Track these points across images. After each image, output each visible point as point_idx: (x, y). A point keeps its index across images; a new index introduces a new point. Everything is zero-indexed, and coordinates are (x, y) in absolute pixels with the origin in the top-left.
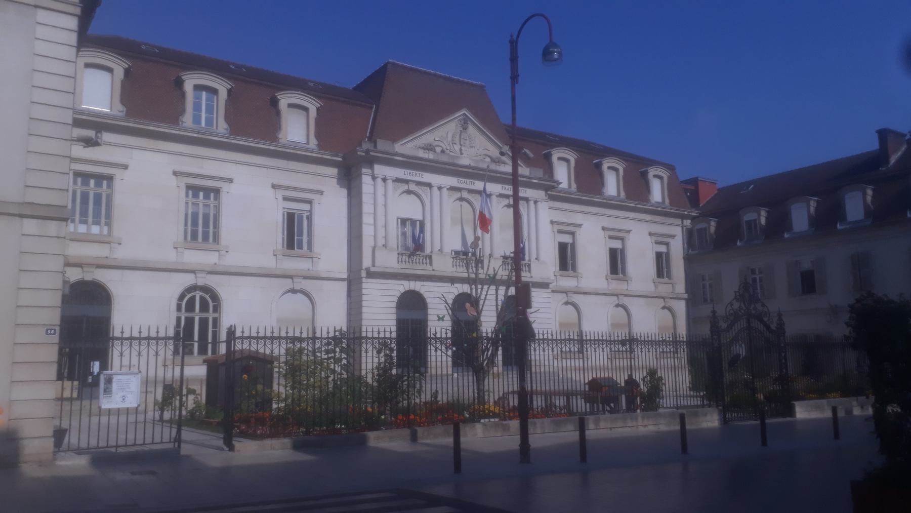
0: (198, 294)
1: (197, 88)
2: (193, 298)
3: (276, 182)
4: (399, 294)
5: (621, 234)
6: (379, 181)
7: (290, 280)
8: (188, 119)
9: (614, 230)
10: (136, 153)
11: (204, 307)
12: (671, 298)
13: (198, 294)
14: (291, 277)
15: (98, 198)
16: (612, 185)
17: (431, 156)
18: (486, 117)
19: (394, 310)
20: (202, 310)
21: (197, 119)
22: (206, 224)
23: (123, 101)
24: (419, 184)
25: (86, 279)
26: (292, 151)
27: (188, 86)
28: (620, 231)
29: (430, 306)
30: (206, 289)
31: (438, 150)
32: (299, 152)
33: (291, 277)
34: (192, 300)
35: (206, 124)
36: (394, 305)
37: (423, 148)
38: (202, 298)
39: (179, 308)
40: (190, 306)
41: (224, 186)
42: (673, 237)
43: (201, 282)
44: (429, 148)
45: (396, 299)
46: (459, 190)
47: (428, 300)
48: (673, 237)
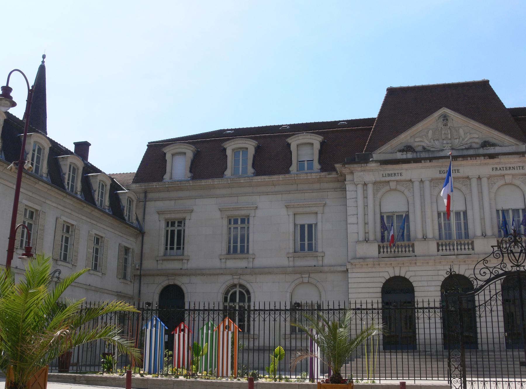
0: (238, 289)
1: (236, 152)
2: (235, 292)
4: (384, 281)
6: (360, 187)
10: (199, 201)
11: (242, 299)
13: (238, 289)
15: (179, 232)
17: (410, 155)
19: (380, 295)
20: (240, 301)
22: (242, 241)
23: (191, 171)
25: (170, 283)
29: (416, 289)
30: (241, 286)
31: (420, 149)
34: (234, 294)
36: (380, 290)
37: (400, 151)
38: (241, 293)
39: (226, 299)
40: (233, 299)
41: (252, 213)
43: (236, 282)
45: (381, 285)
47: (414, 284)
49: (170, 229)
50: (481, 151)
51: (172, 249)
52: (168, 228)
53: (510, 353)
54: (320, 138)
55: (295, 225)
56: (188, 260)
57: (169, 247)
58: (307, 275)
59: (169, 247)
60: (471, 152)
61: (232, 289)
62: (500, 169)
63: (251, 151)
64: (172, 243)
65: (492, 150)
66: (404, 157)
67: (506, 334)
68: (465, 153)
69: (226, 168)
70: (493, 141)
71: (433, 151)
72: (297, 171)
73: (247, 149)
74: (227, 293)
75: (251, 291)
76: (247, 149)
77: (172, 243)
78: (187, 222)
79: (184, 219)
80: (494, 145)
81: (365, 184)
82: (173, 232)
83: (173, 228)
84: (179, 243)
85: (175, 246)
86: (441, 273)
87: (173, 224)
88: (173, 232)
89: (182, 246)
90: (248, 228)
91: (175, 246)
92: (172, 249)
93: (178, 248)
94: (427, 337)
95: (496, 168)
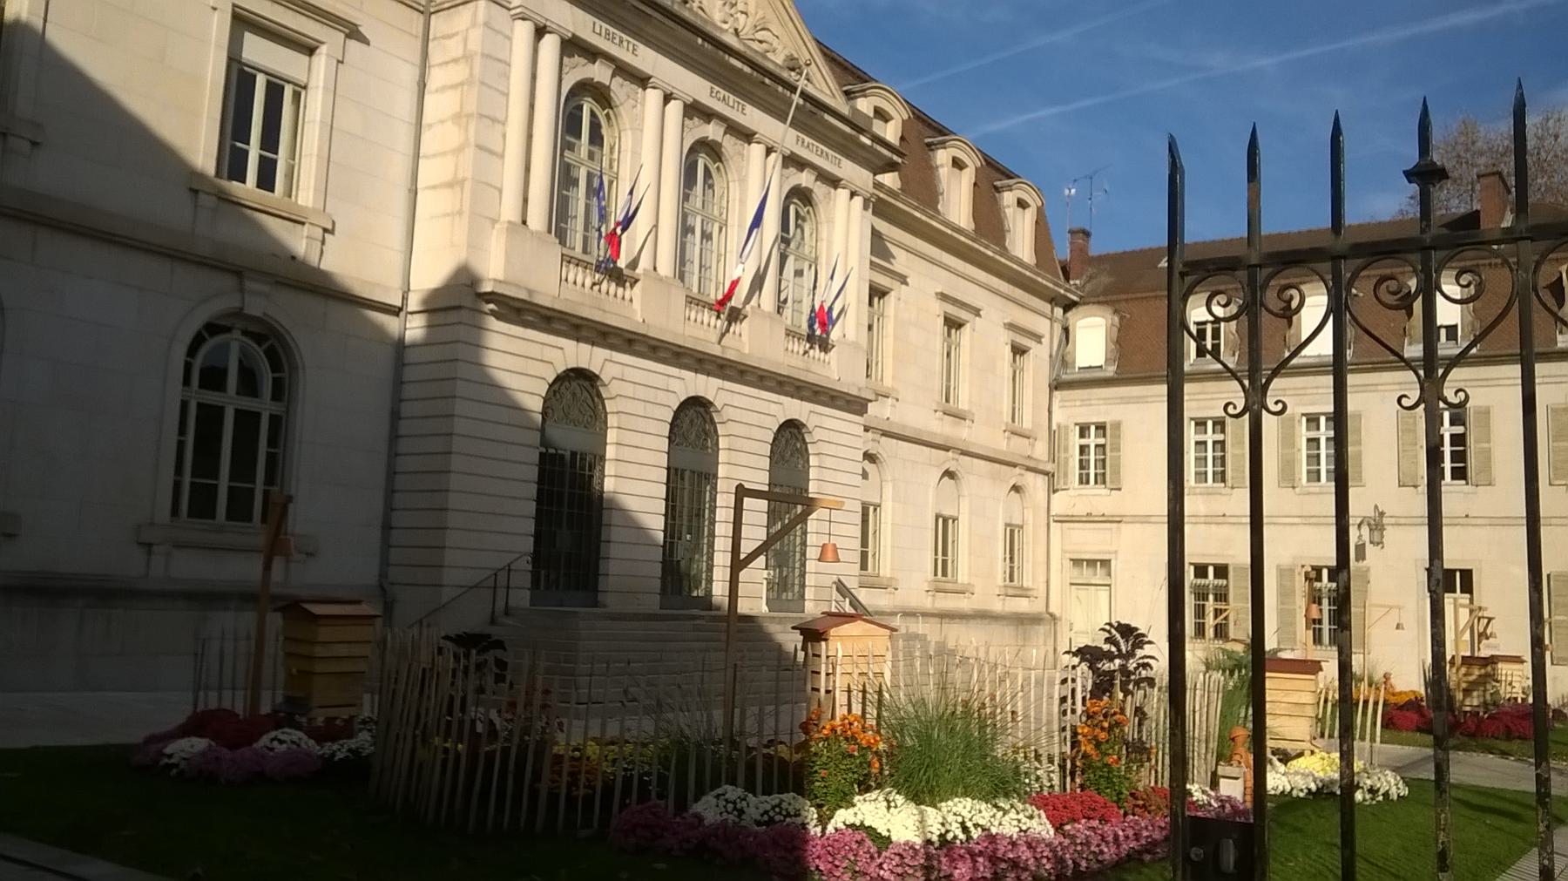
5: (963, 315)
7: (229, 282)
12: (1028, 469)
14: (238, 273)
16: (957, 201)
24: (623, 70)
33: (238, 273)
42: (1038, 338)
46: (708, 115)
48: (1038, 338)
55: (234, 60)
81: (540, 32)
86: (675, 385)
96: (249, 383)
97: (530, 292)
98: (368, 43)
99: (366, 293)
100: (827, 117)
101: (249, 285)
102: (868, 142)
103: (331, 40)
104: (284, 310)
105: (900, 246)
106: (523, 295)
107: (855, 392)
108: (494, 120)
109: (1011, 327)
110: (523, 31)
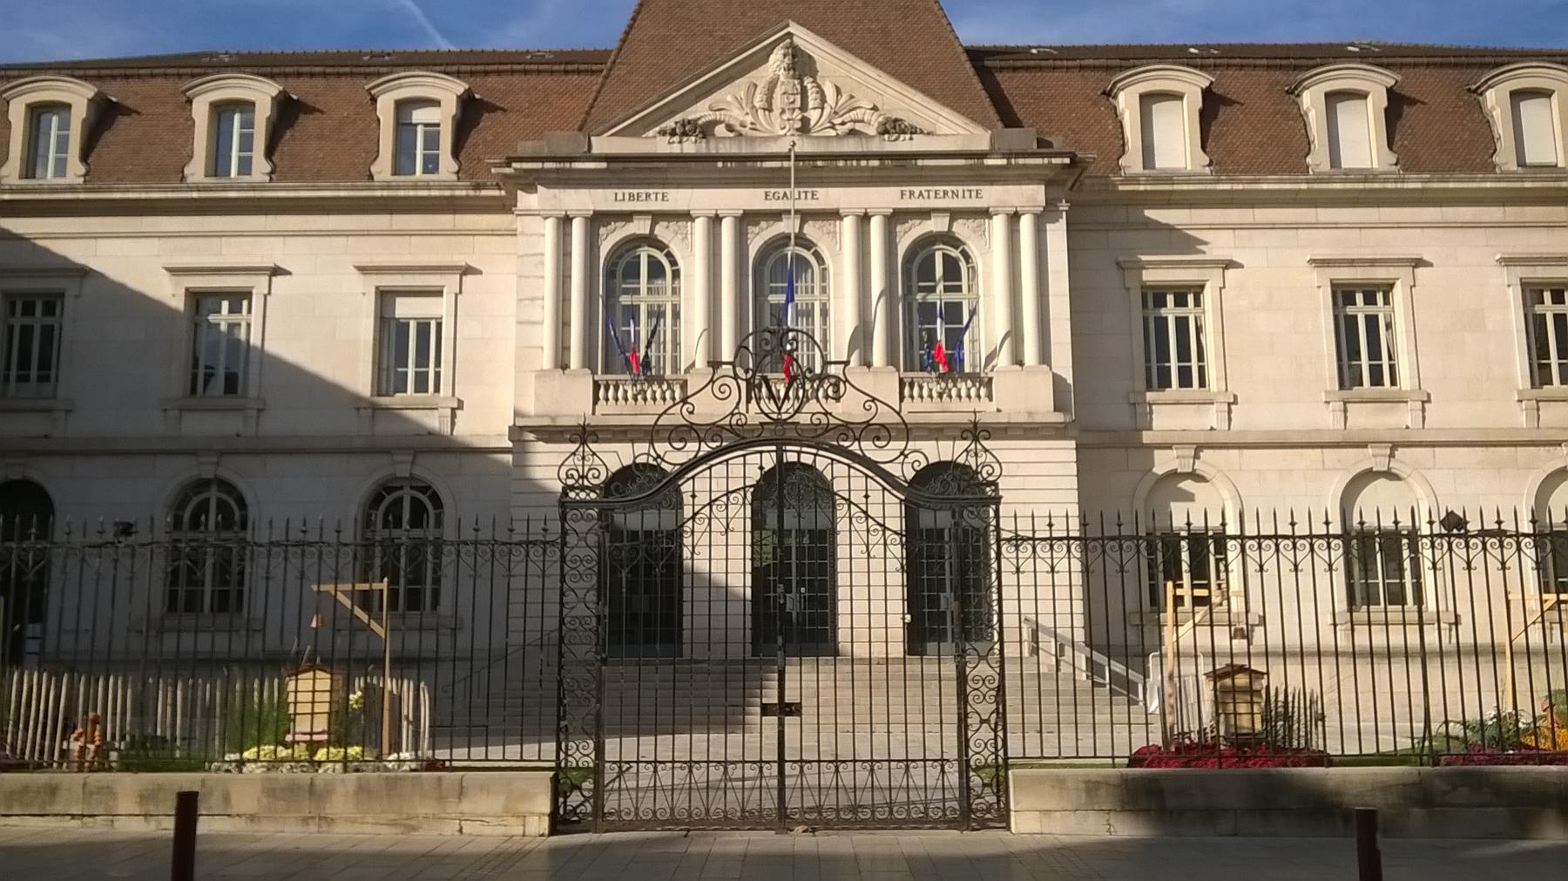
0: (213, 495)
1: (222, 110)
2: (207, 500)
3: (366, 261)
5: (1380, 274)
8: (196, 170)
9: (1352, 263)
14: (387, 451)
15: (48, 332)
17: (690, 146)
18: (896, 32)
21: (217, 166)
26: (385, 193)
27: (200, 111)
28: (1373, 262)
30: (227, 486)
32: (402, 193)
34: (203, 507)
35: (239, 173)
37: (663, 133)
41: (259, 284)
43: (207, 472)
44: (705, 130)
49: (18, 321)
50: (876, 146)
51: (23, 378)
52: (12, 321)
53: (914, 667)
54: (460, 87)
56: (68, 412)
57: (13, 373)
58: (410, 458)
59: (13, 373)
60: (851, 146)
61: (197, 494)
62: (921, 193)
63: (263, 112)
64: (24, 363)
65: (904, 145)
66: (676, 149)
67: (908, 618)
68: (835, 148)
69: (191, 157)
70: (909, 119)
71: (753, 139)
72: (395, 173)
73: (253, 104)
74: (181, 504)
75: (249, 498)
76: (253, 104)
77: (24, 363)
78: (69, 301)
79: (61, 295)
80: (914, 131)
82: (26, 331)
83: (28, 321)
84: (45, 364)
85: (34, 372)
87: (29, 309)
88: (26, 331)
89: (53, 372)
90: (249, 325)
91: (34, 372)
92: (23, 378)
93: (44, 378)
94: (718, 623)
95: (912, 193)
96: (418, 519)
97: (553, 418)
98: (480, 273)
99: (477, 443)
100: (920, 162)
101: (397, 458)
102: (1003, 162)
103: (450, 282)
104: (430, 470)
105: (1212, 227)
106: (546, 422)
107: (1023, 419)
108: (532, 299)
109: (1508, 262)
110: (549, 227)
